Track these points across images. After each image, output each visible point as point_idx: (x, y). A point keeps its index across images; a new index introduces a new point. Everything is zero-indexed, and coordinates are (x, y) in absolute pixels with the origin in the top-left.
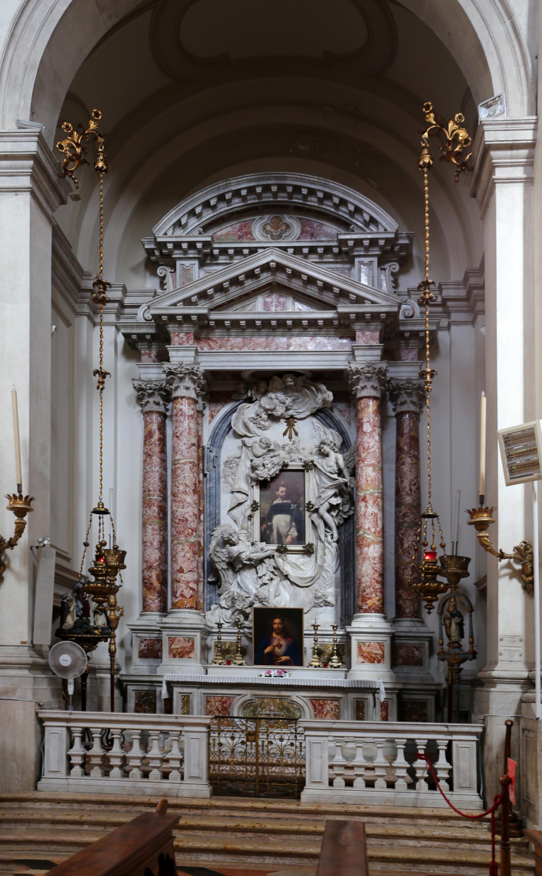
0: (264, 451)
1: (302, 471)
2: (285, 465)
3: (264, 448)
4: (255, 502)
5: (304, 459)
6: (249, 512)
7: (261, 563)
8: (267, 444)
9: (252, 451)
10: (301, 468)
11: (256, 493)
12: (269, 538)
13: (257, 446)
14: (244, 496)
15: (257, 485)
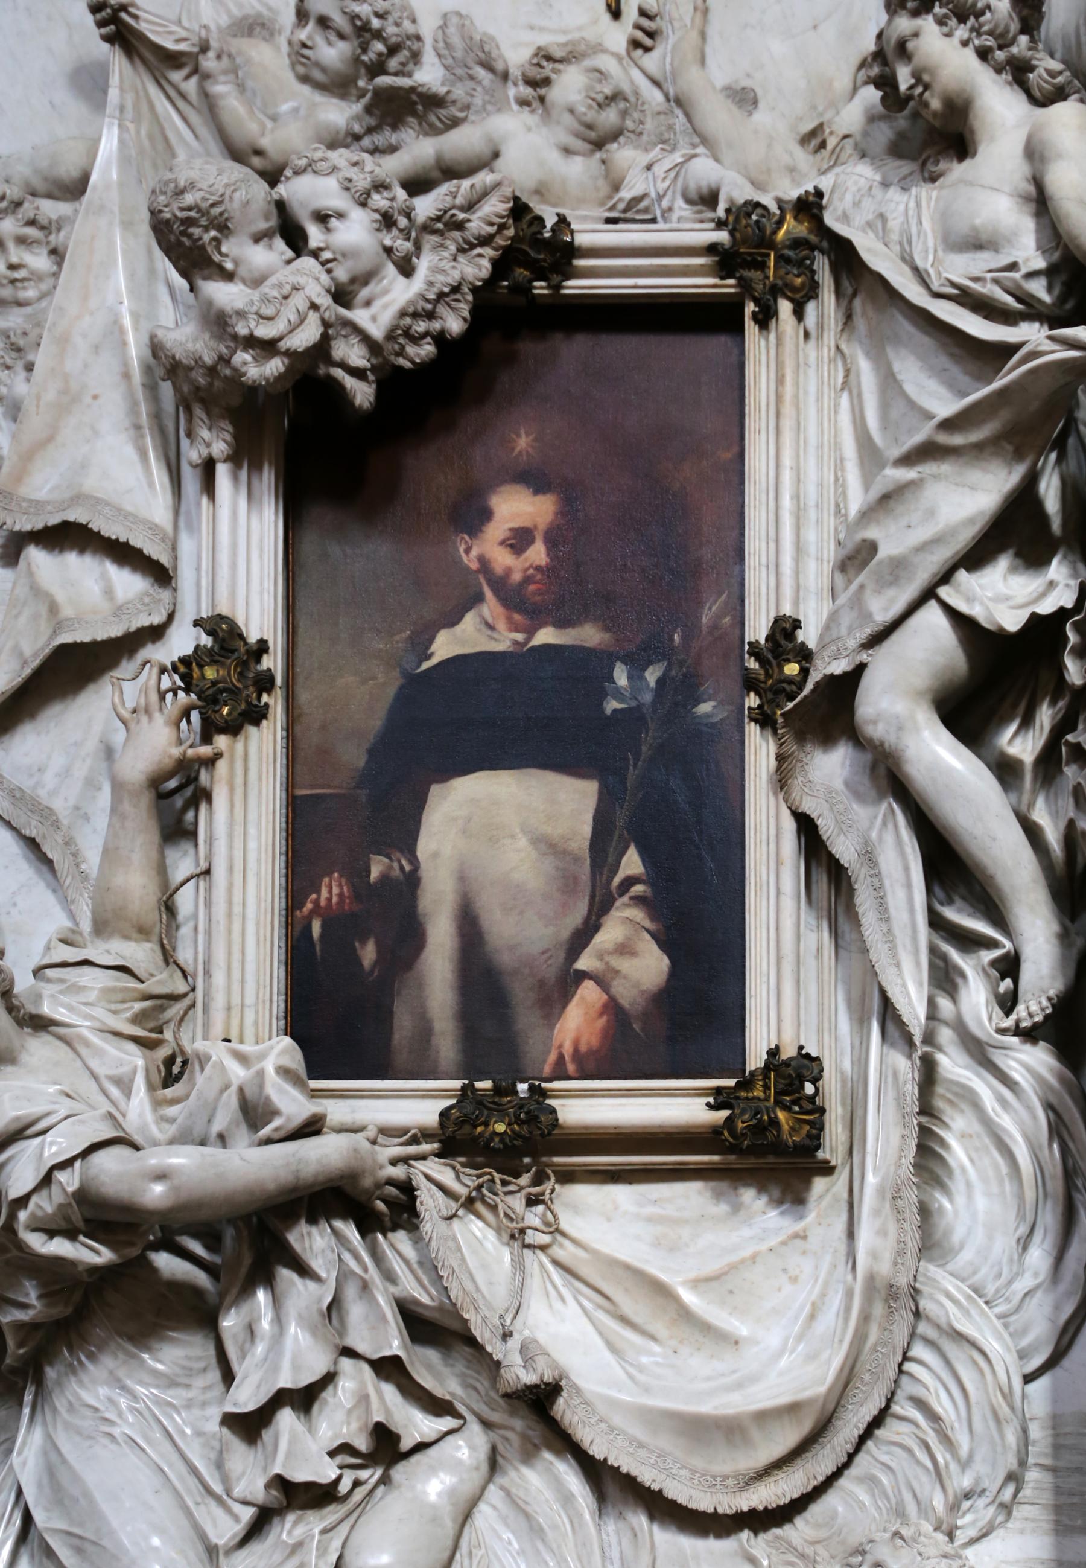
0: (340, 114)
1: (716, 318)
2: (533, 247)
3: (338, 86)
4: (223, 633)
5: (736, 190)
6: (157, 742)
7: (261, 1274)
8: (363, 31)
9: (210, 105)
10: (704, 284)
11: (237, 553)
12: (385, 1017)
13: (269, 59)
14: (129, 584)
15: (244, 455)
